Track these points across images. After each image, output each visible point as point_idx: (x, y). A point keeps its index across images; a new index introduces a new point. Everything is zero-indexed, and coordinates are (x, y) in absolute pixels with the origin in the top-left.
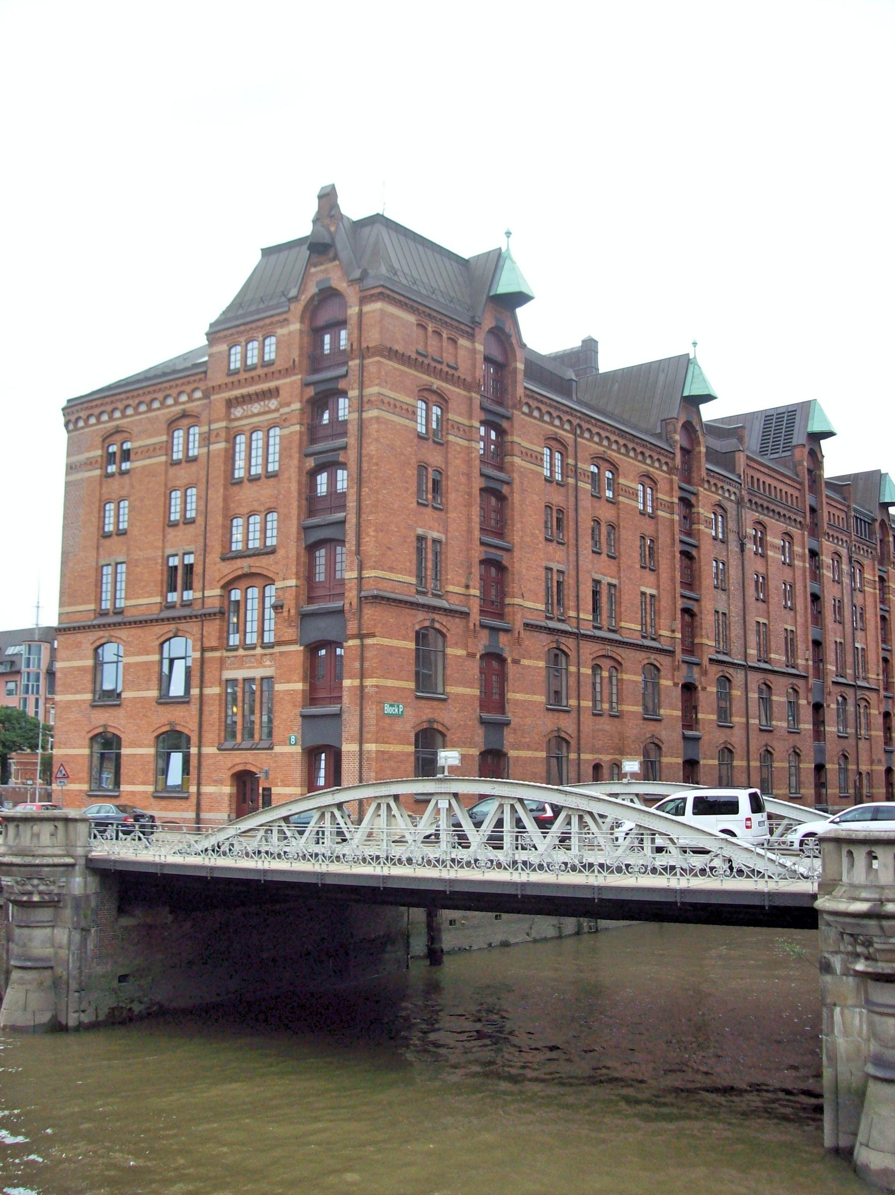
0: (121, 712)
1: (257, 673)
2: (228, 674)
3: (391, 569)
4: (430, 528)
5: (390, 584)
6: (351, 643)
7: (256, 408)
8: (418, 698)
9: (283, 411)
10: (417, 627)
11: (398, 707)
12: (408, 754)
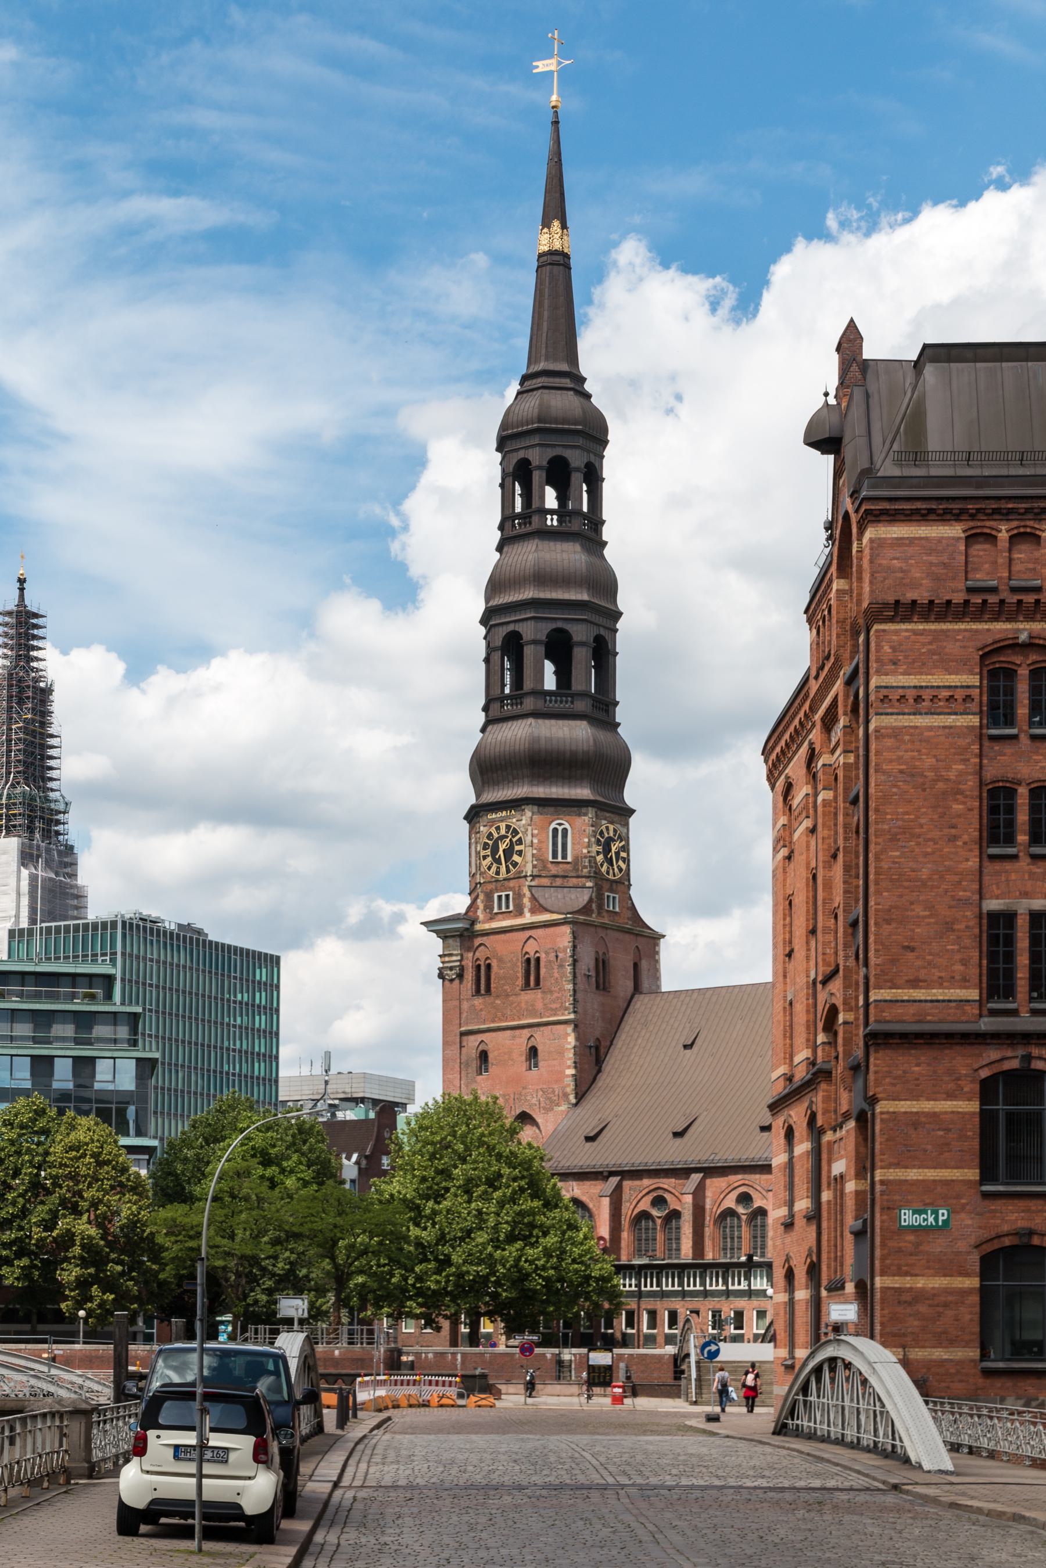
3: (914, 983)
4: (1026, 895)
5: (912, 1009)
8: (986, 1195)
10: (984, 1073)
11: (936, 1213)
12: (968, 1292)
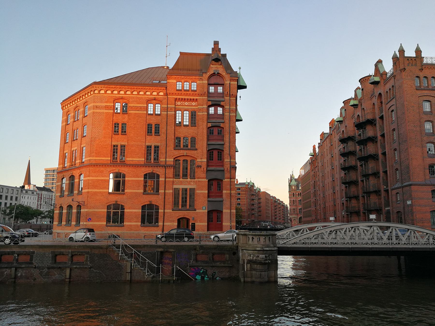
0: (125, 197)
1: (188, 187)
2: (175, 186)
6: (226, 180)
7: (186, 103)
9: (199, 107)
